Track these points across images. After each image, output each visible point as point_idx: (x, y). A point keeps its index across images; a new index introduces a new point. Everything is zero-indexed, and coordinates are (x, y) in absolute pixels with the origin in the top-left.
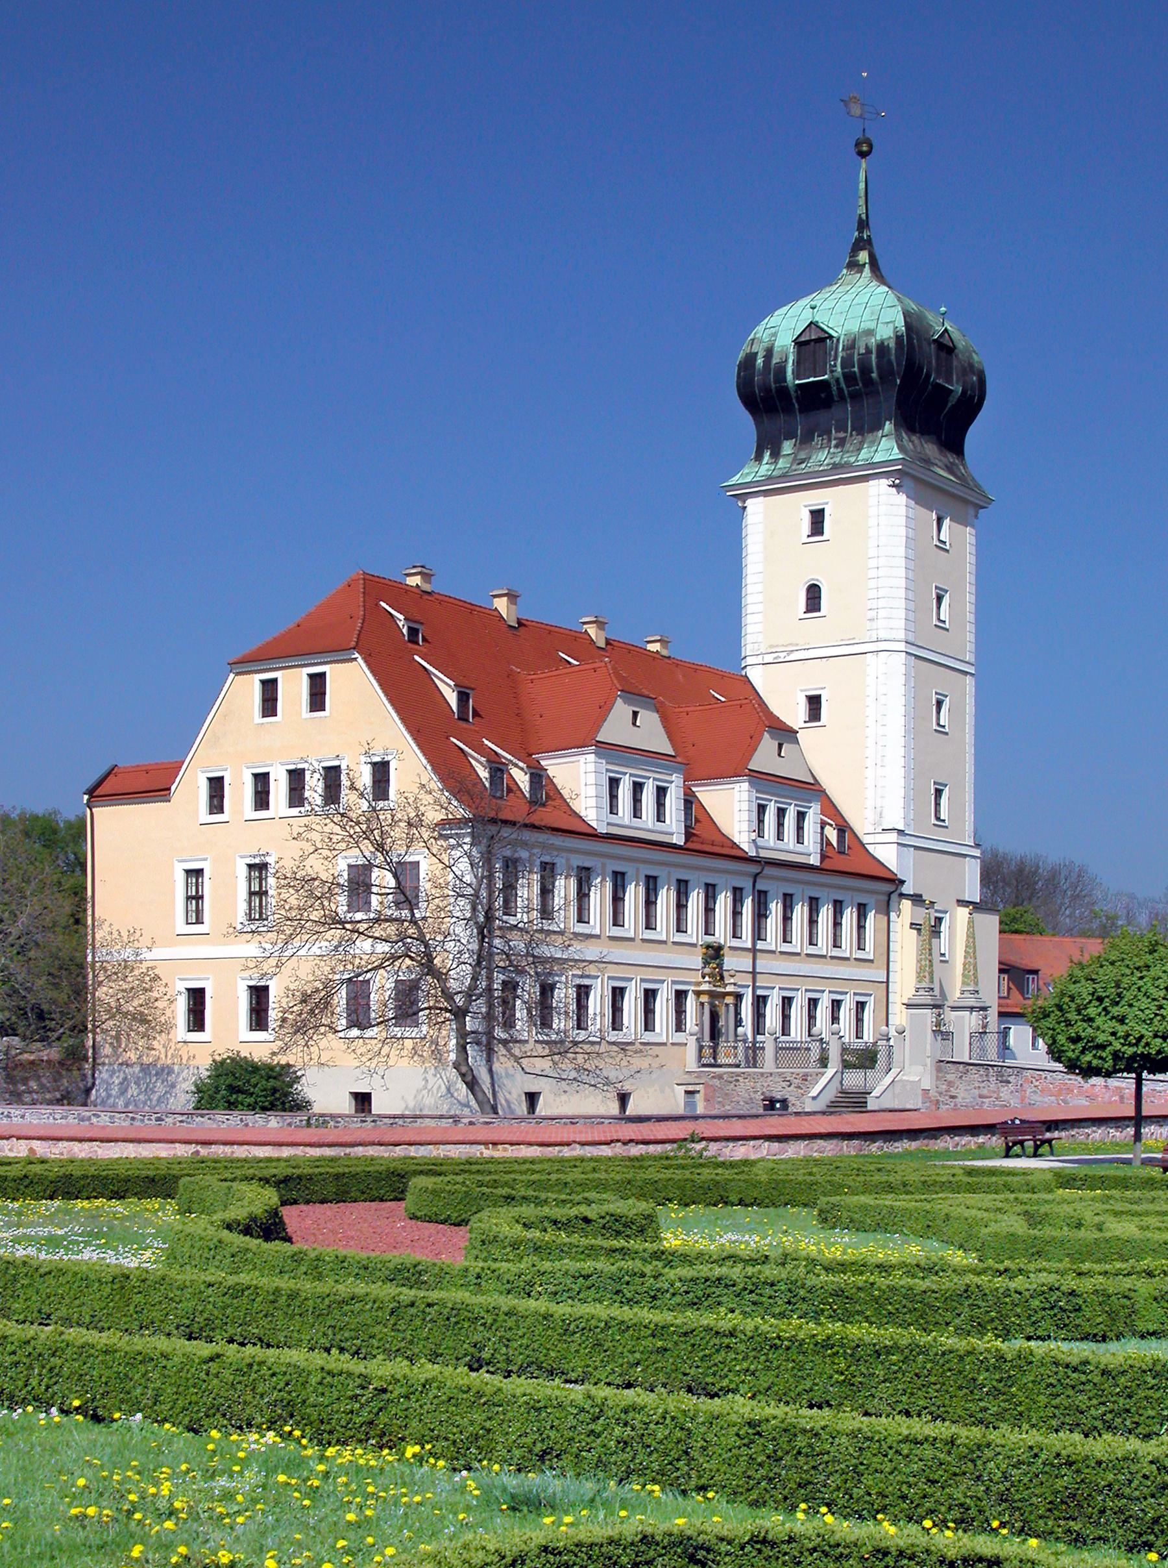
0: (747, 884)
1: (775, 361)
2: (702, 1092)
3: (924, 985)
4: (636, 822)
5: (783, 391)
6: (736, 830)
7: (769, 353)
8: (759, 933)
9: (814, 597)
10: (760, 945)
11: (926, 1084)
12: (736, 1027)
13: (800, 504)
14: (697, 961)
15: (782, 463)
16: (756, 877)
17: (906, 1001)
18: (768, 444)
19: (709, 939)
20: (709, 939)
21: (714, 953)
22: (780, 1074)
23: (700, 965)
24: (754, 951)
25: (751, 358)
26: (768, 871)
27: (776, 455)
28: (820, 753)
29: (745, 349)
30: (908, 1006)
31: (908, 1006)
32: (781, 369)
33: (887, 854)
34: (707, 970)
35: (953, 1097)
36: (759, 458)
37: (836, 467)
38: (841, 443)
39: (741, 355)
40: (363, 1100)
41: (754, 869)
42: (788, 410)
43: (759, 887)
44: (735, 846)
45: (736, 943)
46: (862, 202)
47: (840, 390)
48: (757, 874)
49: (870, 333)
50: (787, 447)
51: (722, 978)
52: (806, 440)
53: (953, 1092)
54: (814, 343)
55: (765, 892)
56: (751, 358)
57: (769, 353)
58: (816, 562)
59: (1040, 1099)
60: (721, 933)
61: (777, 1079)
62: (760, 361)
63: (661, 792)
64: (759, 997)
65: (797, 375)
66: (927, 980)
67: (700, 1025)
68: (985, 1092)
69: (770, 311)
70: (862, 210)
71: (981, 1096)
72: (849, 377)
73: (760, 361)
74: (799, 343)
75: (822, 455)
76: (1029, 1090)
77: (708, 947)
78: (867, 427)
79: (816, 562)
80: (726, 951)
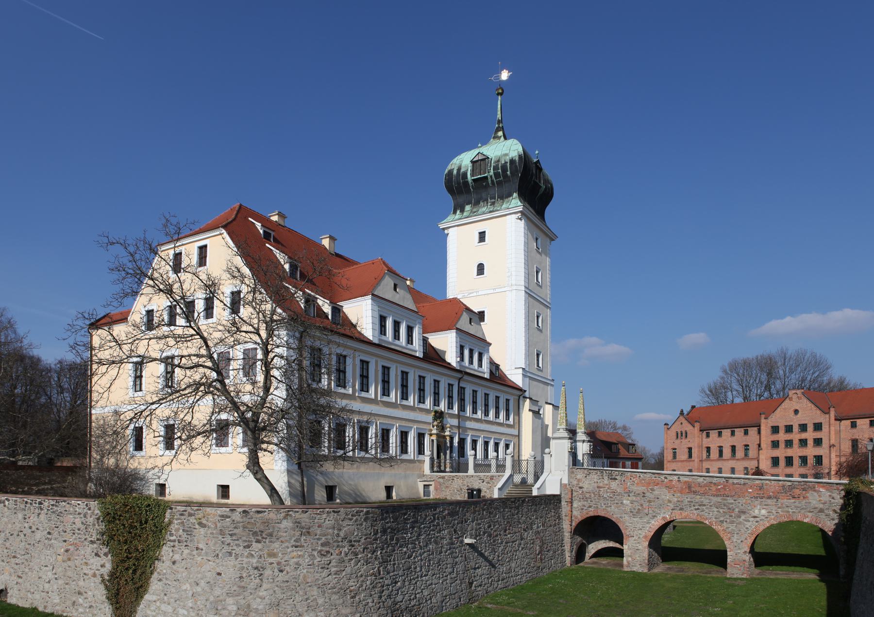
1: (462, 170)
4: (397, 342)
5: (466, 183)
7: (459, 169)
8: (462, 408)
9: (481, 269)
10: (462, 413)
13: (474, 230)
14: (429, 418)
15: (465, 214)
18: (459, 207)
19: (436, 408)
20: (436, 408)
21: (439, 416)
23: (431, 421)
24: (458, 416)
25: (451, 172)
27: (462, 211)
28: (488, 329)
29: (449, 168)
32: (465, 174)
33: (517, 378)
34: (435, 423)
36: (455, 212)
37: (491, 212)
38: (493, 204)
39: (446, 171)
40: (224, 490)
41: (459, 375)
42: (468, 191)
44: (449, 364)
46: (499, 113)
47: (492, 181)
49: (506, 155)
50: (468, 208)
52: (477, 203)
54: (479, 163)
55: (464, 388)
56: (451, 172)
57: (459, 169)
58: (482, 254)
60: (443, 406)
62: (455, 172)
65: (472, 175)
69: (460, 154)
70: (499, 116)
72: (497, 175)
73: (455, 172)
74: (473, 162)
75: (484, 209)
77: (436, 412)
78: (505, 196)
79: (482, 254)
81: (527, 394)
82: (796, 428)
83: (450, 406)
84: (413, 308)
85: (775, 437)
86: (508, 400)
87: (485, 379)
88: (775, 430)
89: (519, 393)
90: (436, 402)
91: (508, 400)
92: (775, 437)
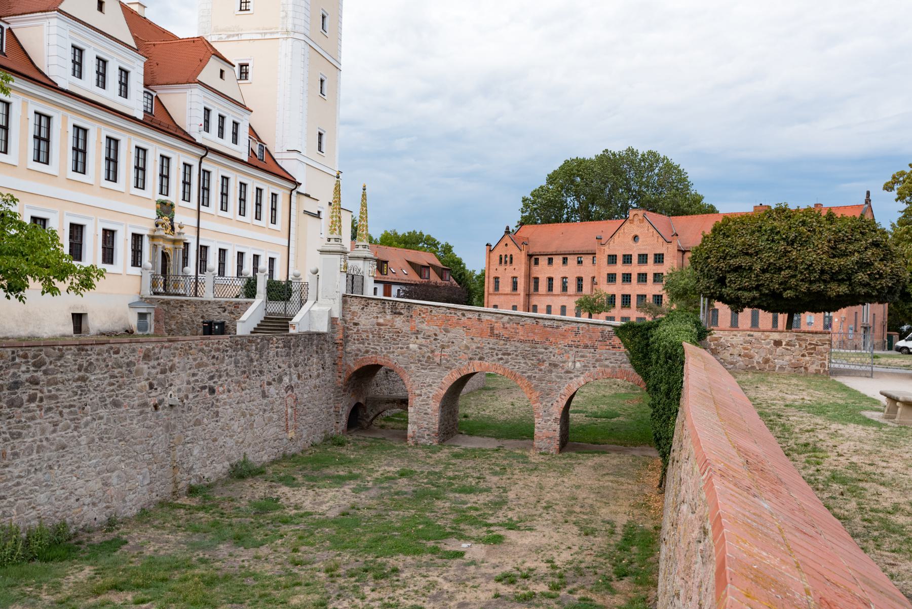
0: (195, 163)
2: (153, 314)
3: (335, 236)
6: (187, 125)
8: (204, 200)
10: (202, 208)
11: (337, 314)
12: (184, 266)
16: (202, 158)
17: (320, 248)
20: (163, 198)
21: (165, 209)
22: (216, 302)
26: (210, 156)
30: (322, 252)
31: (322, 252)
35: (356, 324)
41: (201, 152)
43: (203, 167)
45: (185, 204)
48: (202, 158)
51: (173, 229)
53: (356, 320)
59: (426, 328)
61: (214, 306)
63: (125, 73)
64: (201, 246)
66: (337, 232)
67: (153, 262)
68: (381, 321)
71: (379, 324)
76: (417, 321)
77: (163, 203)
80: (176, 209)
81: (301, 189)
82: (635, 259)
83: (186, 197)
84: (135, 47)
85: (612, 269)
86: (274, 195)
87: (241, 161)
88: (612, 259)
89: (292, 186)
90: (164, 188)
91: (274, 195)
92: (612, 269)
